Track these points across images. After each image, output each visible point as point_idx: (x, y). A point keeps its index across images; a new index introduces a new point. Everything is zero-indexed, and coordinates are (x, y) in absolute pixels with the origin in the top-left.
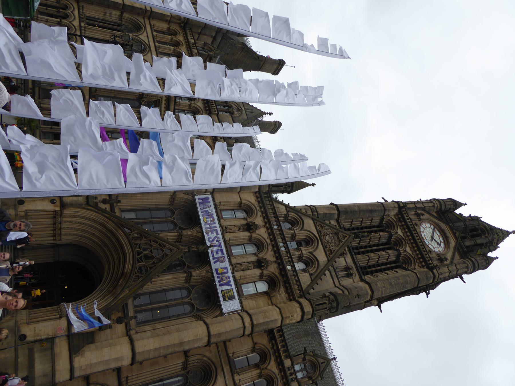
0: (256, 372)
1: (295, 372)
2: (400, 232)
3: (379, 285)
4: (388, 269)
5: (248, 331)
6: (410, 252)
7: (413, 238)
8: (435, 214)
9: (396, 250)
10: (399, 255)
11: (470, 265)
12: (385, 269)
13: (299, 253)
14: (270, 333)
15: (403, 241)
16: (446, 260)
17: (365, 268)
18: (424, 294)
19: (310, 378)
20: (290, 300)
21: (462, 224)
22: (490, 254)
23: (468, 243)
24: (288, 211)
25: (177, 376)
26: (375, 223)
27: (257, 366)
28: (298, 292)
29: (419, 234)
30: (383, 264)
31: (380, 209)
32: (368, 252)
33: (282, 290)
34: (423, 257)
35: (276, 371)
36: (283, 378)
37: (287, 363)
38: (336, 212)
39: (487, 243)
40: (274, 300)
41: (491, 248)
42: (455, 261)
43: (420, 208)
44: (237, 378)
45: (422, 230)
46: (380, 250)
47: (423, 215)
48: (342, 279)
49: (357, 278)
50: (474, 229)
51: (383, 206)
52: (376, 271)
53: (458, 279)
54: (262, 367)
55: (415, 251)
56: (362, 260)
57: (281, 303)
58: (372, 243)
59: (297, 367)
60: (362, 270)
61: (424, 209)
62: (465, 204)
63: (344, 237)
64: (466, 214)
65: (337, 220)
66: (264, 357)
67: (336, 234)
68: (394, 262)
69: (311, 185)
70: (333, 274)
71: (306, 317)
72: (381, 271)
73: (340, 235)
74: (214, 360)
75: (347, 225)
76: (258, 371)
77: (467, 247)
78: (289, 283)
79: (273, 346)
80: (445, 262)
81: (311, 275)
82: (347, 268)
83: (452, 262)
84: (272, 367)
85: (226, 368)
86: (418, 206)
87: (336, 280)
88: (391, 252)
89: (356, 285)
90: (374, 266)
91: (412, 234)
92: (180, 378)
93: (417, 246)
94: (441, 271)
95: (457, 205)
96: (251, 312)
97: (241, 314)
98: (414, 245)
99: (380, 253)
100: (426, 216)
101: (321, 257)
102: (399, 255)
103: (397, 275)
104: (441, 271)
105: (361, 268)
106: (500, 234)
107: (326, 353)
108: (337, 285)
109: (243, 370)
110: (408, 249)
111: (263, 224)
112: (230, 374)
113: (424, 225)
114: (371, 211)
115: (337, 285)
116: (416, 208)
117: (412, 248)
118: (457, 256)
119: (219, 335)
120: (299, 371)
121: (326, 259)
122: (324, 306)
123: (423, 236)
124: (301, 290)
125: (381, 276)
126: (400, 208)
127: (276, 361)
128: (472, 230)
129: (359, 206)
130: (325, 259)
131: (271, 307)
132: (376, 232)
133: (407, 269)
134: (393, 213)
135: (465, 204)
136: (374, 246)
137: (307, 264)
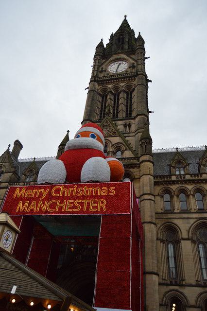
0: (175, 198)
1: (180, 175)
2: (110, 86)
3: (140, 109)
4: (131, 100)
5: (152, 198)
6: (124, 84)
7: (116, 79)
8: (104, 61)
9: (121, 92)
10: (124, 91)
11: (140, 50)
12: (131, 103)
13: (111, 153)
14: (156, 184)
16: (134, 63)
17: (127, 114)
18: (149, 84)
19: (185, 167)
20: (139, 167)
21: (114, 47)
22: (136, 36)
23: (126, 47)
25: (168, 247)
26: (100, 99)
27: (172, 197)
28: (135, 160)
30: (127, 103)
31: (92, 94)
32: (117, 110)
33: (131, 170)
34: (129, 77)
35: (177, 186)
36: (182, 183)
37: (174, 178)
39: (129, 36)
40: (136, 177)
41: (132, 34)
42: (136, 59)
44: (176, 211)
45: (112, 72)
46: (118, 102)
47: (102, 68)
48: (131, 130)
49: (132, 121)
50: (119, 40)
52: (131, 108)
53: (146, 61)
54: (173, 194)
55: (124, 80)
56: (122, 115)
57: (140, 173)
58: (112, 106)
59: (177, 173)
60: (127, 117)
61: (99, 67)
62: (102, 39)
63: (107, 122)
64: (108, 42)
66: (168, 191)
67: (104, 126)
68: (127, 96)
69: (68, 133)
70: (127, 135)
71: (152, 160)
72: (131, 105)
73: (105, 124)
74: (163, 223)
75: (98, 118)
76: (175, 197)
77: (129, 48)
78: (128, 165)
79: (162, 184)
80: (135, 65)
81: (126, 150)
82: (125, 126)
83: (136, 61)
84: (174, 187)
85: (170, 216)
86: (96, 69)
87: (131, 134)
88: (121, 95)
89: (136, 123)
90: (127, 108)
91: (114, 79)
92: (169, 246)
93: (121, 78)
94: (140, 69)
95: (101, 44)
96: (141, 193)
97: (141, 199)
98: (120, 80)
99: (120, 102)
100: (103, 66)
101: (116, 140)
102: (124, 91)
103: (136, 96)
104: (140, 69)
105: (127, 117)
106: (125, 25)
107: (171, 153)
108: (133, 134)
109: (172, 206)
112: (172, 214)
113: (109, 70)
114: (93, 100)
115: (133, 134)
116: (97, 71)
117: (122, 82)
118: (133, 56)
119: (151, 216)
120: (180, 172)
121: (118, 137)
122: (147, 146)
124: (134, 158)
125: (134, 106)
126: (95, 81)
127: (171, 185)
128: (119, 42)
129: (87, 106)
131: (141, 180)
132: (106, 101)
133: (134, 90)
134: (97, 86)
135: (102, 39)
136: (114, 104)
137: (118, 150)
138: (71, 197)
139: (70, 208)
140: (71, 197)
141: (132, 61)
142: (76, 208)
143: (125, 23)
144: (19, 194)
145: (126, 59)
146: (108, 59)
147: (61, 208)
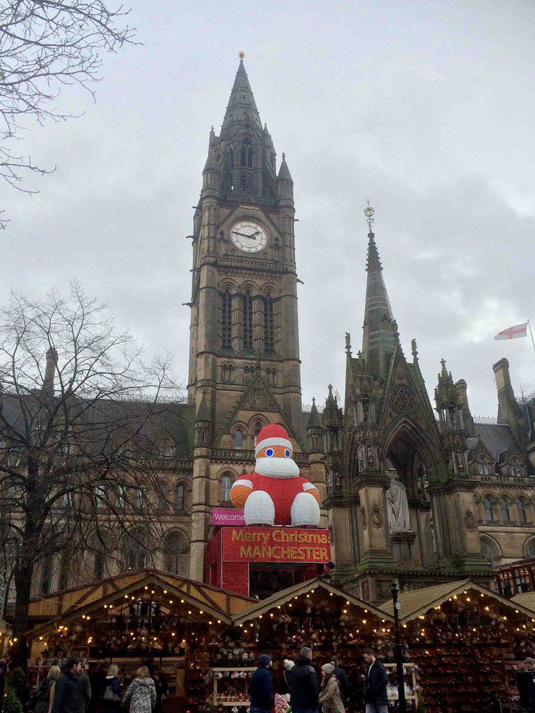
15: (249, 283)
16: (277, 239)
24: (229, 434)
29: (244, 255)
38: (211, 355)
43: (215, 234)
47: (222, 233)
51: (210, 288)
65: (217, 356)
80: (280, 243)
83: (282, 234)
100: (223, 228)
110: (260, 283)
111: (241, 466)
115: (281, 391)
118: (273, 217)
123: (245, 249)
130: (277, 415)
133: (278, 299)
138: (293, 544)
139: (295, 555)
140: (293, 544)
141: (276, 234)
142: (300, 555)
143: (241, 74)
144: (238, 538)
145: (264, 224)
146: (231, 213)
147: (286, 555)
